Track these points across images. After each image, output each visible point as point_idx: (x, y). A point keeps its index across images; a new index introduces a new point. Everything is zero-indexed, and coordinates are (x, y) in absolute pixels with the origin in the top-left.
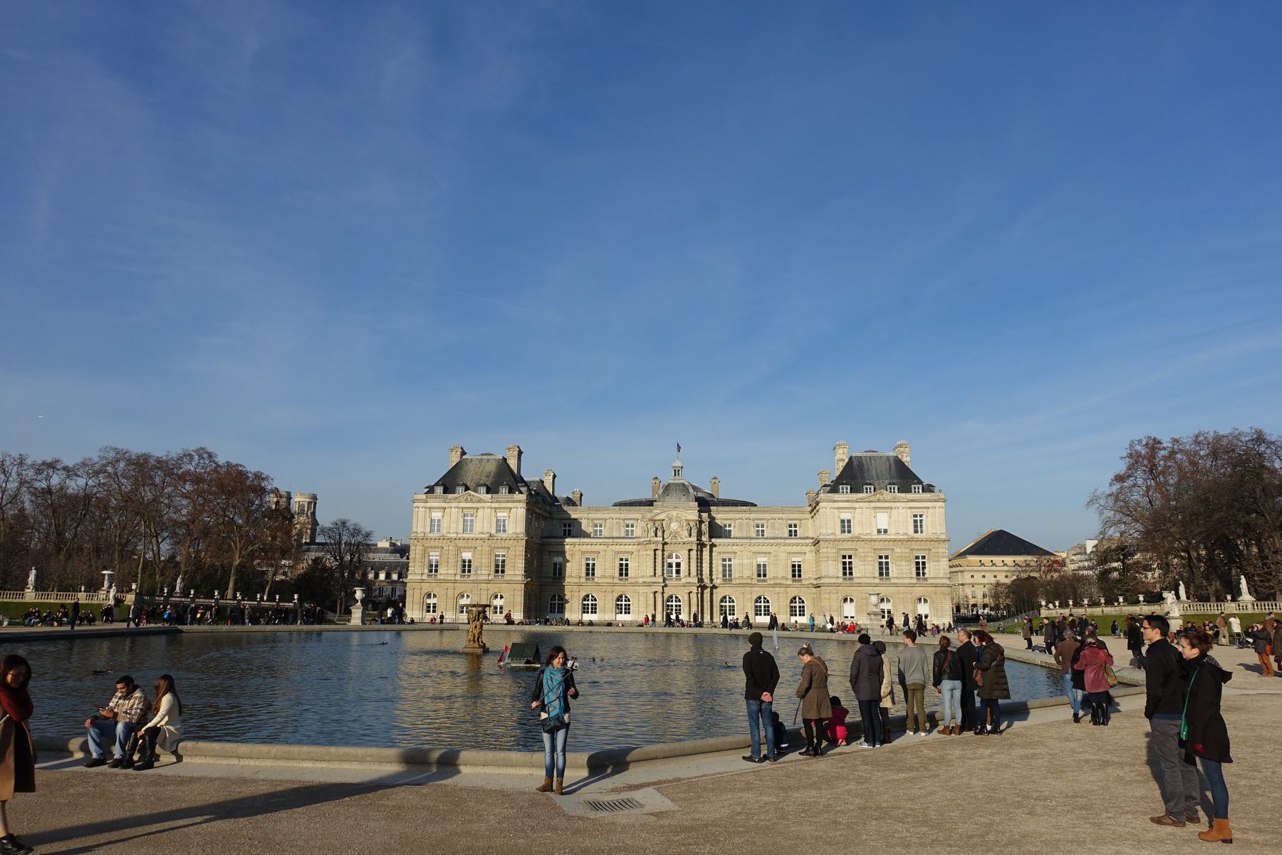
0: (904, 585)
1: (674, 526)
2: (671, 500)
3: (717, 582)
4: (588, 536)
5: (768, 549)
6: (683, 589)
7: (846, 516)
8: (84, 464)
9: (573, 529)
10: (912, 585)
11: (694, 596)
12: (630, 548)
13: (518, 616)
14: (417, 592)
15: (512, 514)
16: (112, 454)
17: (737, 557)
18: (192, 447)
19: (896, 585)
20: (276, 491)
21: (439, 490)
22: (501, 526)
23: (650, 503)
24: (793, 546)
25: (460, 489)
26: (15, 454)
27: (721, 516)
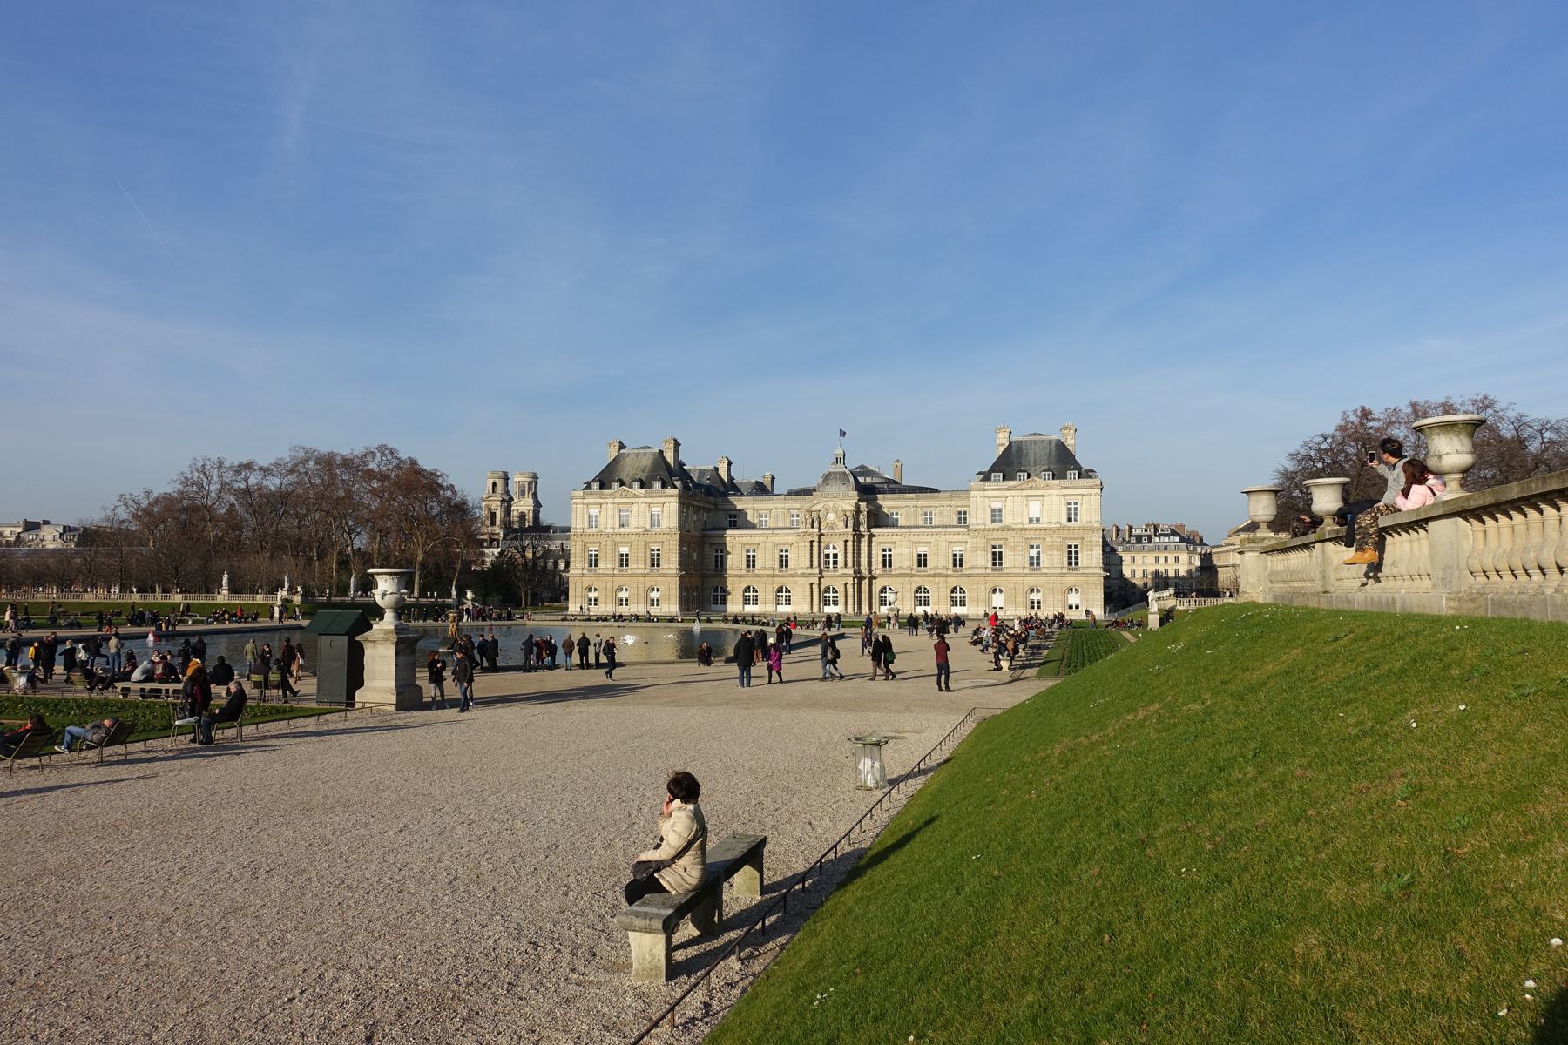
0: (1054, 575)
1: (831, 517)
2: (833, 488)
3: (876, 572)
4: (754, 527)
5: (929, 538)
6: (840, 578)
7: (996, 505)
8: (277, 464)
9: (737, 520)
10: (1063, 575)
11: (850, 588)
12: (790, 539)
13: (672, 608)
14: (579, 587)
15: (662, 511)
16: (301, 454)
17: (899, 544)
18: (373, 443)
19: (1046, 575)
20: (451, 487)
21: (596, 486)
22: (655, 521)
23: (808, 492)
24: (959, 535)
25: (616, 485)
26: (214, 458)
27: (887, 503)
